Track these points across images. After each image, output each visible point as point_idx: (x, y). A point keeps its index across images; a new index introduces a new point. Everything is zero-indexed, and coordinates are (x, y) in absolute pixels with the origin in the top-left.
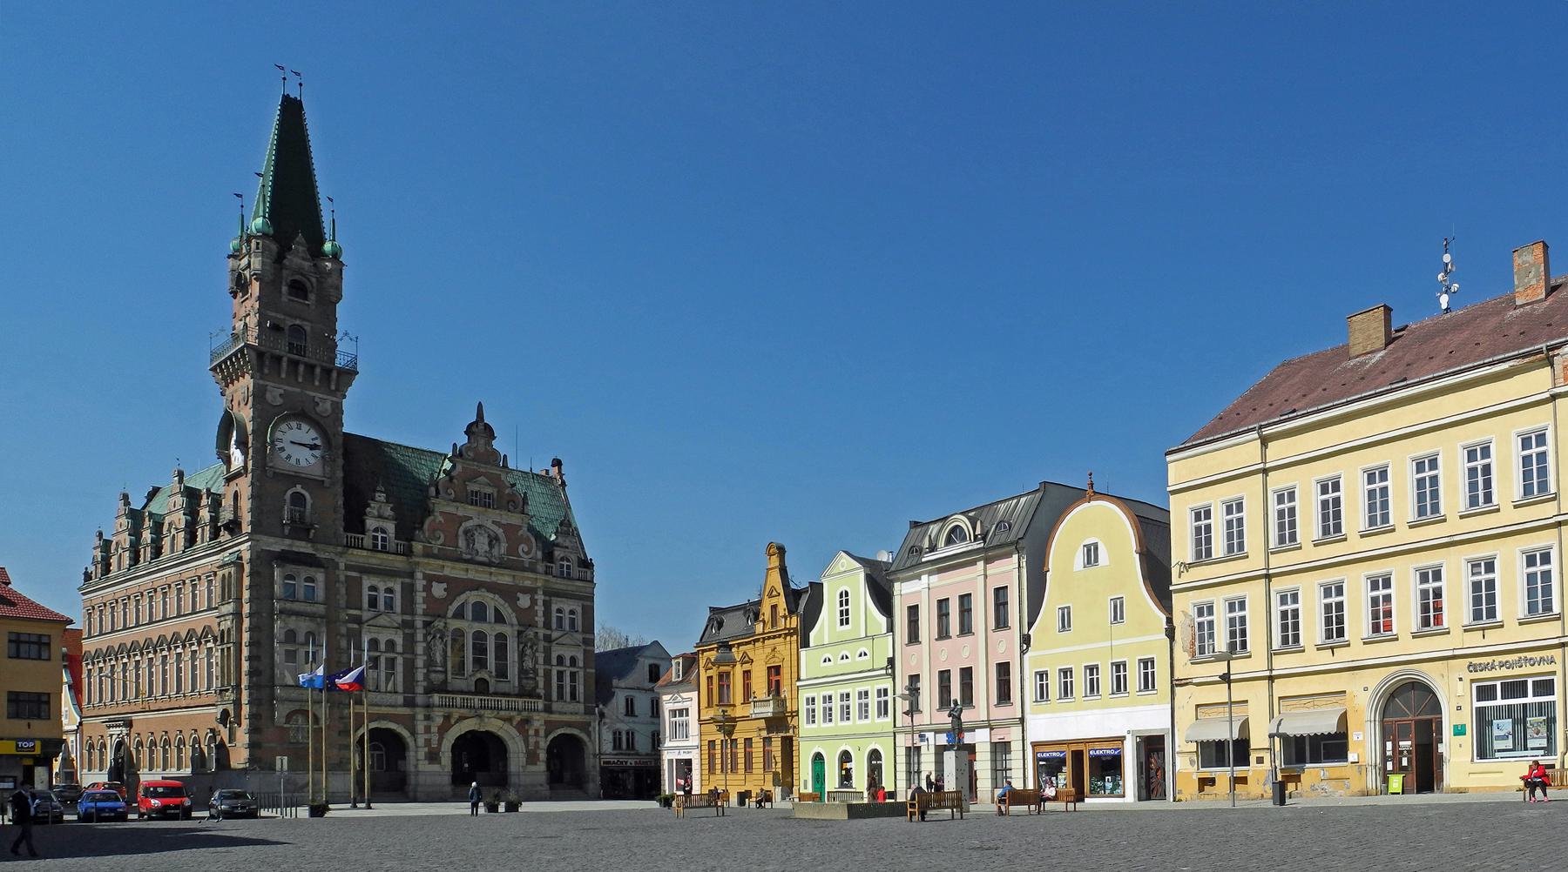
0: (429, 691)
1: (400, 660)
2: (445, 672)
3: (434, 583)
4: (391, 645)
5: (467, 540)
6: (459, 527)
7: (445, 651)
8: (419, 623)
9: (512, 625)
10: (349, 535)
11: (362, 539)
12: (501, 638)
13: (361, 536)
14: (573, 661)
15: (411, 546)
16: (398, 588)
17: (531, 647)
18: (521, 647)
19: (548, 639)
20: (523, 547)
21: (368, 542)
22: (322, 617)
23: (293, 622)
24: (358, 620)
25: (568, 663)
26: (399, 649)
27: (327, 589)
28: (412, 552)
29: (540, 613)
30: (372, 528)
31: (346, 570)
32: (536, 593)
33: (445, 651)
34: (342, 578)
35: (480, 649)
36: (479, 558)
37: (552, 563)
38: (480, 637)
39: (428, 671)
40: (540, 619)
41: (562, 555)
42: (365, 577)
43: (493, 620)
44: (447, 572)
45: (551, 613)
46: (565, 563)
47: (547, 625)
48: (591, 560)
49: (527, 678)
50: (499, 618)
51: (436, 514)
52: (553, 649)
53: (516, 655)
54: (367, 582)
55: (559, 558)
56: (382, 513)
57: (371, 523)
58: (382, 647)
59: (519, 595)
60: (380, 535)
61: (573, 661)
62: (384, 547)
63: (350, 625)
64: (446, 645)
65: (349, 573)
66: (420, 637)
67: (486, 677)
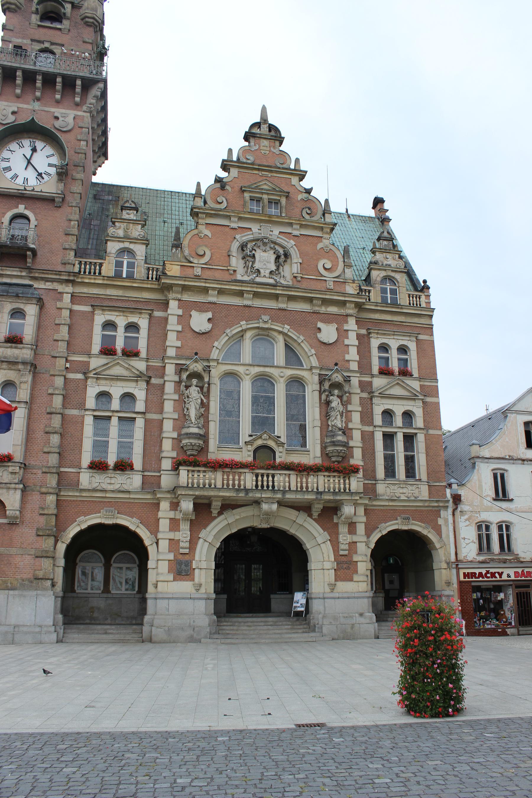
0: (176, 466)
1: (140, 422)
2: (205, 437)
3: (194, 313)
5: (243, 258)
6: (232, 242)
7: (205, 405)
8: (170, 369)
10: (83, 260)
11: (101, 265)
13: (100, 261)
14: (408, 415)
16: (143, 323)
17: (340, 397)
18: (324, 397)
19: (365, 386)
20: (324, 263)
22: (24, 363)
25: (398, 421)
26: (140, 406)
27: (39, 327)
30: (114, 251)
31: (72, 302)
32: (347, 322)
34: (66, 313)
37: (371, 286)
39: (179, 435)
40: (353, 354)
41: (382, 275)
43: (282, 362)
44: (212, 298)
45: (370, 352)
46: (389, 287)
48: (425, 282)
49: (334, 444)
51: (200, 227)
52: (375, 400)
53: (317, 410)
54: (100, 319)
55: (379, 279)
56: (129, 233)
57: (113, 247)
58: (115, 404)
59: (320, 325)
61: (408, 415)
63: (71, 376)
64: (207, 395)
65: (76, 308)
66: (169, 388)
67: (271, 443)
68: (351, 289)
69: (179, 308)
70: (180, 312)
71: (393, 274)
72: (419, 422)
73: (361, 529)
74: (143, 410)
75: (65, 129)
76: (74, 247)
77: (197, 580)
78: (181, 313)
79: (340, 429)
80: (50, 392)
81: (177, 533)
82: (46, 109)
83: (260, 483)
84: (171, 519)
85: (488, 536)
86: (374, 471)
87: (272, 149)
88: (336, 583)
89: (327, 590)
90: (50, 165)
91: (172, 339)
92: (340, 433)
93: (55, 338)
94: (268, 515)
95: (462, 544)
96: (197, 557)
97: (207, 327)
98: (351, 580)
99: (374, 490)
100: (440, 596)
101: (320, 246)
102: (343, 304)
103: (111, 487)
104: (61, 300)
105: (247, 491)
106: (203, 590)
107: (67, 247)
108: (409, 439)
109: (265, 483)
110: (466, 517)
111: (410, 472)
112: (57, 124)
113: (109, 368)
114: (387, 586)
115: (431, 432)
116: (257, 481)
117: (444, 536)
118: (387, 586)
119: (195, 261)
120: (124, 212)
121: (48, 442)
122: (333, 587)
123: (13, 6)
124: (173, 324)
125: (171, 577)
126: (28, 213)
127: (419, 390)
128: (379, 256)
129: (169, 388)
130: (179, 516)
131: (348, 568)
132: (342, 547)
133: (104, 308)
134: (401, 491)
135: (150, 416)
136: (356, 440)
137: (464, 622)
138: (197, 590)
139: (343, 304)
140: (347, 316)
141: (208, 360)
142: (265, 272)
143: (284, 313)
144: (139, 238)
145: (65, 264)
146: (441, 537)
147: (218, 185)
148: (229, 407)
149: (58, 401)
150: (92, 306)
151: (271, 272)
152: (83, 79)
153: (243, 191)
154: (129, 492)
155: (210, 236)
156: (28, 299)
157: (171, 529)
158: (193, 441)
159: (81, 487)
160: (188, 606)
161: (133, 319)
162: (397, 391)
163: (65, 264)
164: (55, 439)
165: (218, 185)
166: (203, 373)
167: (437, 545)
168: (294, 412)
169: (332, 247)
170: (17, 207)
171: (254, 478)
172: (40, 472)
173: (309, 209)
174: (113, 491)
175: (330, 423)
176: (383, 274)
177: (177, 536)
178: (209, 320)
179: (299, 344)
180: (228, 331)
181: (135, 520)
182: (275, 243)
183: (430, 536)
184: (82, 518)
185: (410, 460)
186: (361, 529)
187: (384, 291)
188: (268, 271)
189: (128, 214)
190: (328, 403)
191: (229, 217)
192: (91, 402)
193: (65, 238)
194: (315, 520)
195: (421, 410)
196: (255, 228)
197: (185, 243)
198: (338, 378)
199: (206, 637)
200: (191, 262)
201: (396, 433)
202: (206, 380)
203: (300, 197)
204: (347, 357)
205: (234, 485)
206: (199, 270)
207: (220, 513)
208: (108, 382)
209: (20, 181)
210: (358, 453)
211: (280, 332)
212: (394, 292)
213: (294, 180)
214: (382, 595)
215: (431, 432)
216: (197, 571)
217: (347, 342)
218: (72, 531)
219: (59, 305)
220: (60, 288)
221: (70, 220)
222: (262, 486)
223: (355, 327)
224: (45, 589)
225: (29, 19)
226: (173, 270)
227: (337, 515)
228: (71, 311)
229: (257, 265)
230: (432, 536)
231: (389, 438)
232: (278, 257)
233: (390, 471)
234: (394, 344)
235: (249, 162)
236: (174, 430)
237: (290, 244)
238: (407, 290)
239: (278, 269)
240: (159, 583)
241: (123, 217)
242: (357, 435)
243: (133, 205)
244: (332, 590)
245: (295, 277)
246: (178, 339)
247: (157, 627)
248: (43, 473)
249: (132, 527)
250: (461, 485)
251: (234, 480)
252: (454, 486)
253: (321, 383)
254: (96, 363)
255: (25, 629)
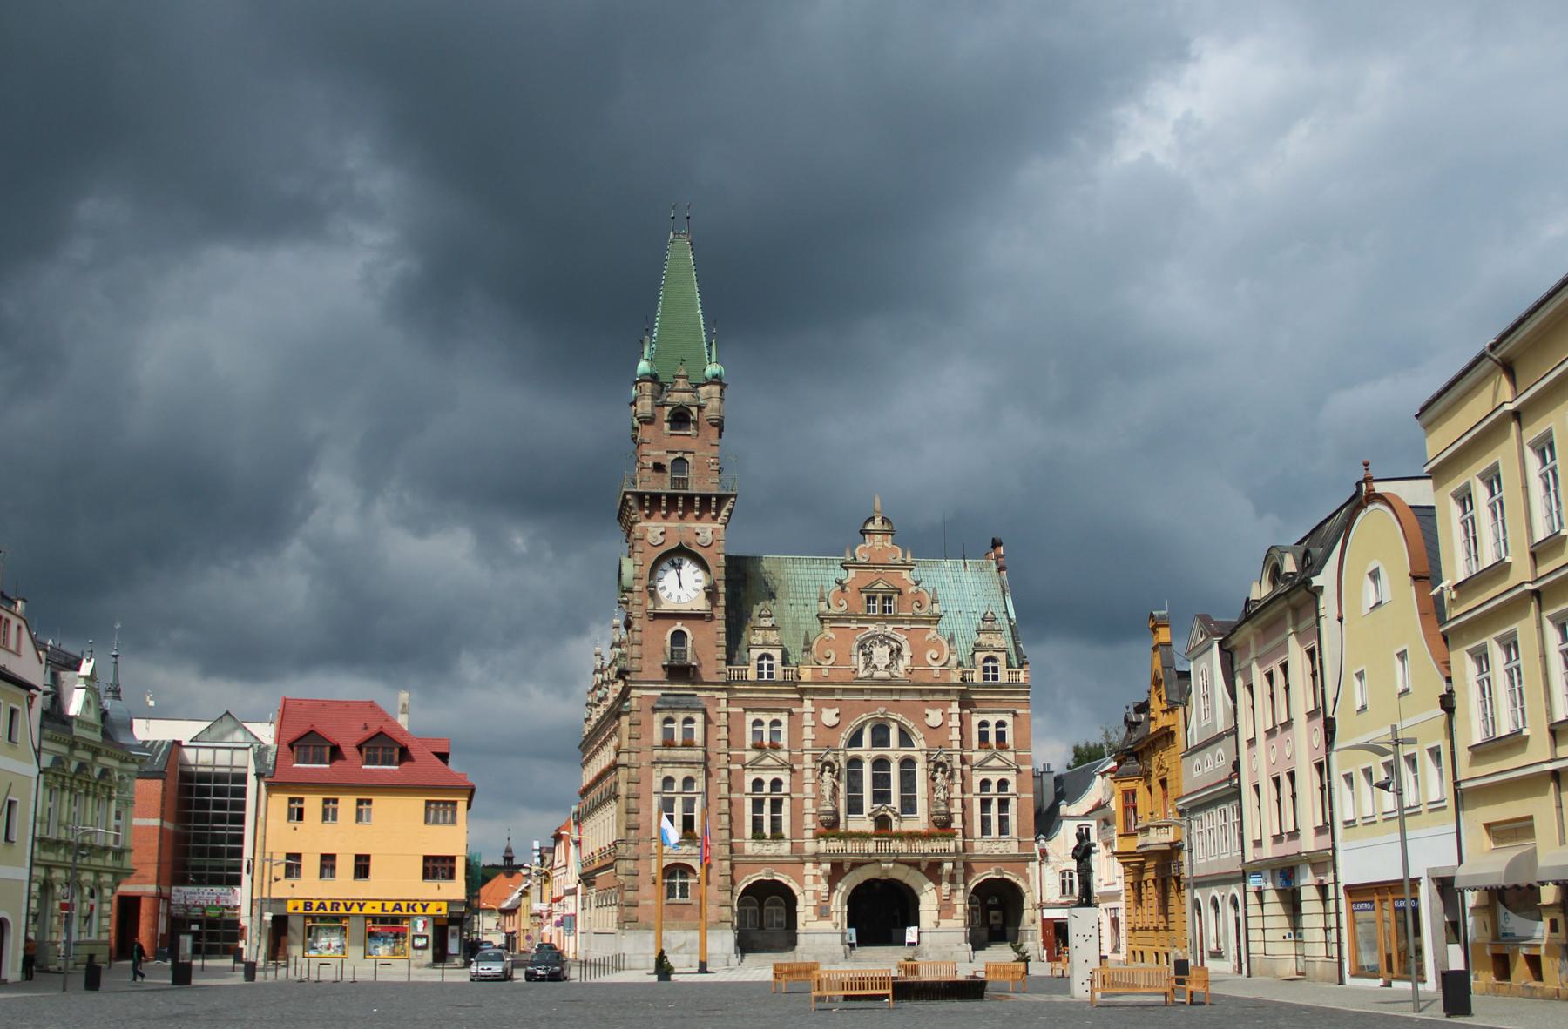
2: (836, 813)
3: (824, 710)
4: (776, 784)
6: (852, 642)
7: (835, 788)
8: (808, 758)
9: (921, 750)
11: (747, 670)
12: (907, 763)
13: (746, 667)
15: (798, 672)
16: (784, 718)
17: (943, 772)
18: (930, 774)
20: (931, 653)
21: (752, 674)
22: (698, 763)
23: (668, 772)
24: (741, 760)
25: (994, 788)
26: (785, 788)
28: (800, 678)
29: (956, 732)
30: (756, 657)
32: (950, 706)
33: (835, 788)
35: (881, 780)
36: (877, 675)
38: (881, 764)
42: (748, 713)
47: (964, 742)
50: (905, 739)
51: (825, 630)
55: (981, 660)
59: (927, 711)
60: (765, 662)
61: (1003, 784)
62: (770, 675)
64: (838, 778)
65: (731, 710)
66: (808, 774)
67: (888, 813)
68: (955, 677)
69: (812, 706)
70: (813, 710)
71: (995, 654)
72: (1012, 788)
73: (960, 878)
74: (788, 791)
75: (705, 545)
76: (725, 657)
77: (834, 920)
78: (813, 711)
79: (943, 801)
80: (718, 782)
81: (819, 886)
82: (688, 525)
83: (879, 848)
84: (814, 875)
85: (1071, 883)
86: (972, 831)
87: (885, 544)
88: (941, 921)
89: (933, 925)
90: (697, 581)
91: (808, 733)
92: (943, 803)
93: (718, 738)
94: (887, 870)
95: (1046, 888)
96: (834, 903)
97: (835, 721)
98: (951, 918)
99: (972, 847)
100: (1027, 931)
101: (927, 637)
102: (946, 692)
103: (768, 853)
104: (718, 705)
105: (870, 855)
106: (839, 927)
107: (719, 658)
108: (1003, 804)
109: (883, 848)
110: (1051, 867)
111: (1003, 830)
112: (699, 540)
113: (762, 760)
114: (992, 921)
115: (1023, 796)
116: (877, 846)
117: (1030, 882)
118: (992, 921)
119: (823, 663)
120: (762, 619)
121: (720, 821)
122: (938, 924)
123: (648, 420)
124: (808, 720)
125: (815, 918)
126: (684, 629)
127: (1012, 759)
128: (983, 638)
129: (808, 774)
130: (819, 873)
131: (949, 910)
132: (944, 893)
133: (753, 710)
134: (994, 846)
135: (793, 795)
136: (956, 808)
137: (1045, 951)
138: (836, 928)
139: (946, 692)
140: (951, 701)
141: (838, 750)
142: (881, 666)
143: (897, 703)
144: (776, 643)
145: (718, 673)
146: (1028, 883)
147: (839, 588)
148: (854, 784)
149: (724, 788)
150: (744, 709)
151: (887, 667)
152: (716, 495)
153: (861, 592)
154: (782, 857)
155: (834, 637)
156: (696, 710)
157: (814, 883)
158: (829, 817)
159: (746, 853)
160: (829, 938)
161: (776, 716)
162: (994, 763)
163: (718, 673)
164: (725, 818)
165: (839, 588)
166: (834, 762)
167: (1025, 890)
168: (907, 785)
169: (938, 637)
170: (676, 625)
171: (875, 844)
172: (716, 844)
173: (919, 602)
174: (770, 856)
175: (935, 796)
176: (985, 655)
177: (819, 887)
178: (837, 715)
179: (910, 730)
180: (852, 723)
181: (787, 876)
182: (889, 638)
183: (1018, 882)
184: (749, 876)
185: (1003, 821)
186: (960, 878)
187: (986, 669)
188: (884, 665)
189: (765, 621)
190: (934, 779)
191: (849, 621)
192: (748, 788)
193: (716, 649)
194: (923, 873)
195: (1015, 778)
196: (872, 627)
197: (814, 647)
198: (942, 758)
199: (842, 961)
200: (820, 665)
201: (992, 799)
202: (837, 767)
203: (913, 589)
204: (950, 738)
205: (860, 850)
206: (827, 670)
207: (850, 870)
208: (760, 772)
209: (674, 599)
210: (958, 819)
211: (894, 720)
212: (995, 669)
213: (906, 574)
214: (987, 929)
215: (1023, 796)
216: (834, 913)
217: (950, 724)
218: (741, 887)
219: (718, 709)
220: (718, 695)
221: (718, 633)
222: (881, 850)
223: (958, 710)
224: (728, 929)
225: (662, 429)
226: (806, 674)
227: (939, 867)
228: (728, 713)
229: (875, 661)
230: (1021, 883)
231: (986, 804)
232: (892, 652)
233: (986, 829)
234: (992, 720)
235: (865, 560)
236: (813, 807)
237: (902, 638)
238: (1007, 667)
239: (891, 663)
240: (807, 923)
241: (762, 625)
242: (958, 803)
243: (769, 613)
244: (937, 927)
245: (907, 670)
246: (813, 733)
247: (808, 954)
248: (720, 844)
249: (785, 882)
250: (1047, 840)
251: (860, 846)
252: (1042, 841)
253: (929, 762)
254: (750, 756)
255: (717, 957)
